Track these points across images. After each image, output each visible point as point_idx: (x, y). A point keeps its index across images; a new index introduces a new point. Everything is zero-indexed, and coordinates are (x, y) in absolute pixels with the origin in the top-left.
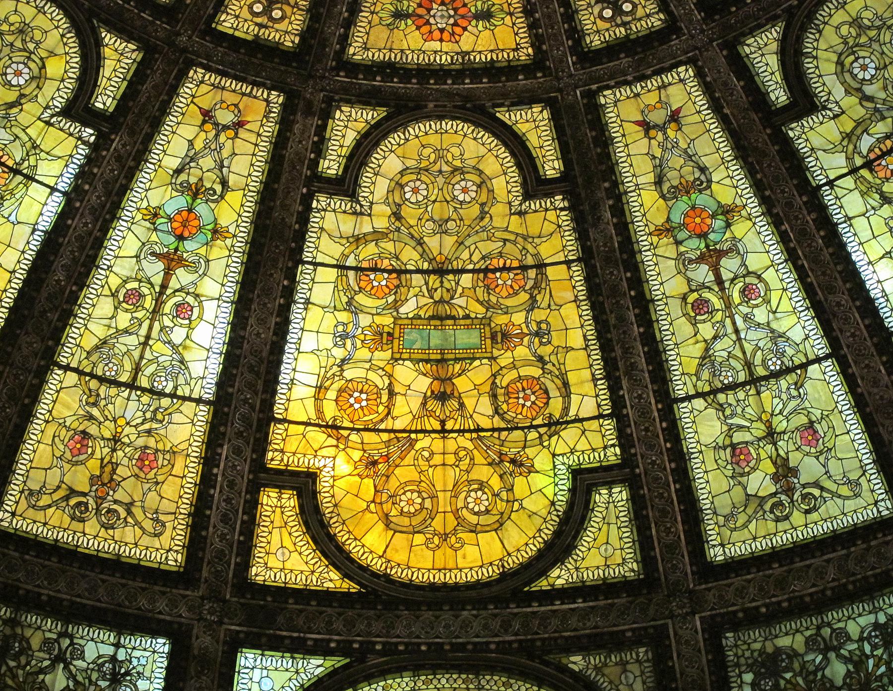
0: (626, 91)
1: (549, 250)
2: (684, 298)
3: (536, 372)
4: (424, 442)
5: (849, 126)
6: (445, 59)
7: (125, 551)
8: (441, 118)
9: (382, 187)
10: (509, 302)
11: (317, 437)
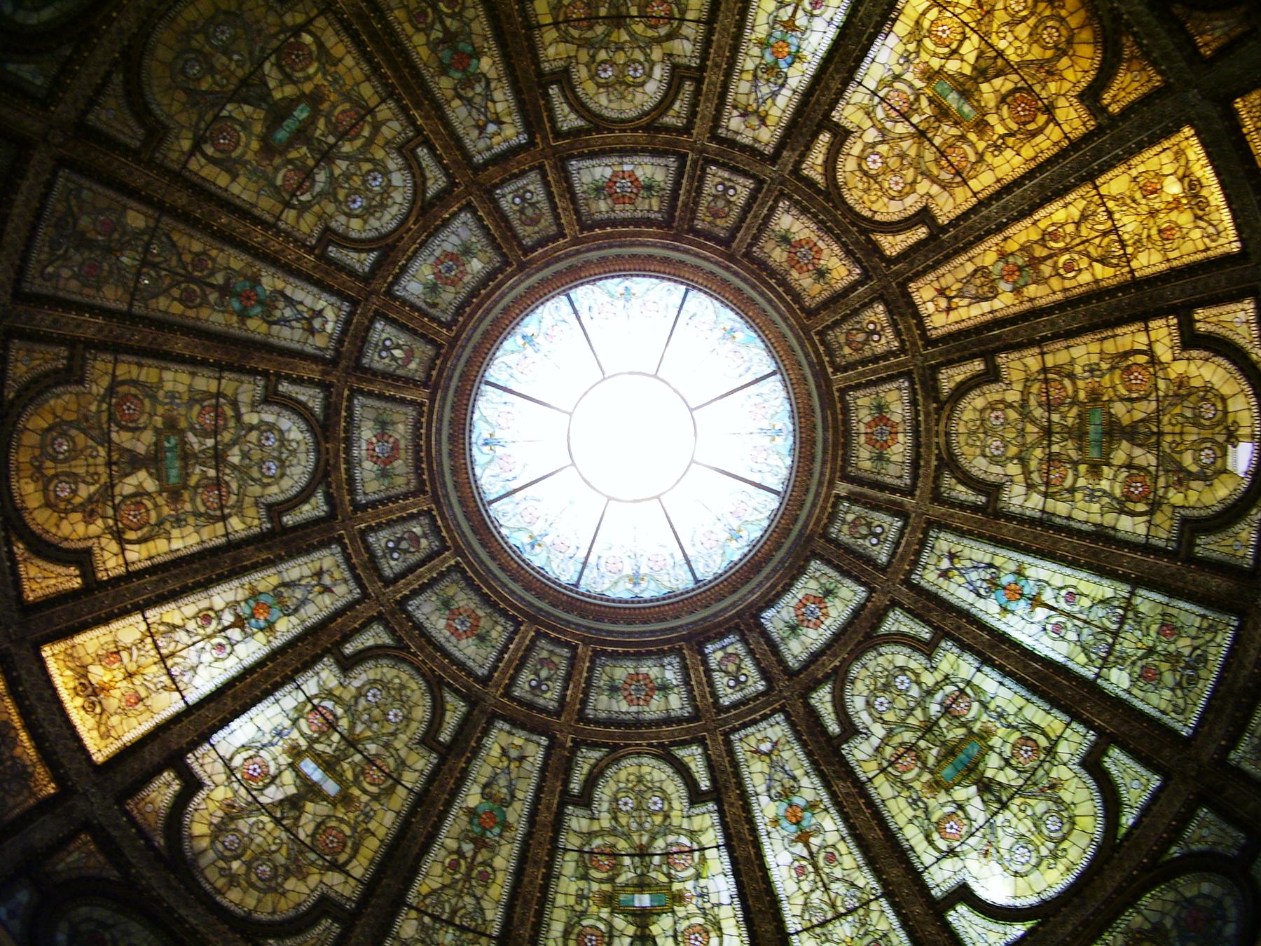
0: (340, 559)
1: (235, 523)
2: (211, 609)
3: (153, 520)
4: (102, 452)
5: (337, 693)
6: (355, 452)
9: (269, 418)
10: (199, 501)
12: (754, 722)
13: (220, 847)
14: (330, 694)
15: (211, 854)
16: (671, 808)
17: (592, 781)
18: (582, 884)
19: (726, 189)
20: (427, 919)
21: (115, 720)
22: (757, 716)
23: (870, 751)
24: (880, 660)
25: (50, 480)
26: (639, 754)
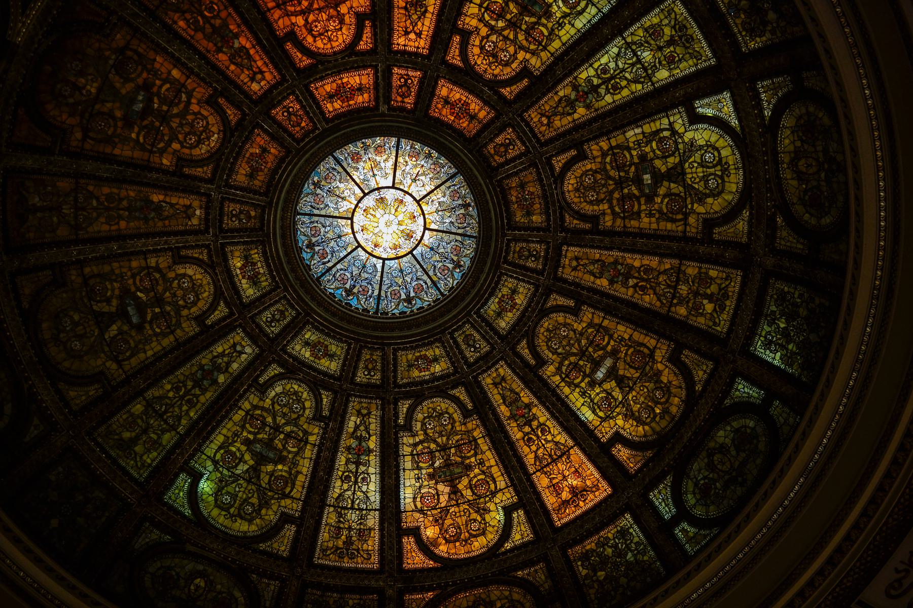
2: (523, 439)
3: (482, 477)
4: (452, 510)
5: (557, 365)
8: (432, 397)
9: (419, 425)
11: (417, 515)
12: (532, 130)
13: (648, 420)
14: (559, 369)
15: (653, 424)
16: (591, 169)
17: (583, 217)
18: (643, 215)
19: (233, 216)
21: (588, 483)
24: (479, 62)
25: (470, 534)
26: (563, 193)
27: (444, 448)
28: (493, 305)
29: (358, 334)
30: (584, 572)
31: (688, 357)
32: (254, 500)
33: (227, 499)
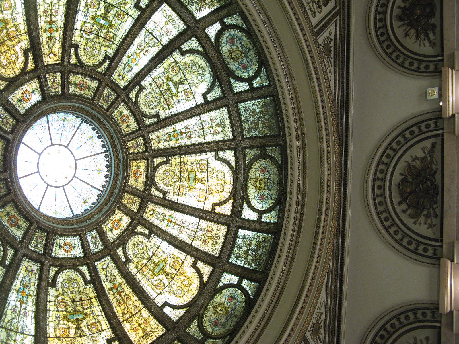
0: (153, 145)
4: (209, 185)
6: (145, 174)
7: (224, 236)
11: (207, 202)
12: (53, 64)
13: (203, 77)
16: (84, 46)
17: (103, 62)
18: (116, 33)
19: (37, 246)
20: (159, 40)
22: (53, 66)
23: (22, 42)
24: (9, 73)
26: (88, 66)
27: (180, 179)
28: (124, 127)
29: (114, 201)
30: (257, 133)
31: (185, 47)
32: (183, 278)
33: (179, 292)
